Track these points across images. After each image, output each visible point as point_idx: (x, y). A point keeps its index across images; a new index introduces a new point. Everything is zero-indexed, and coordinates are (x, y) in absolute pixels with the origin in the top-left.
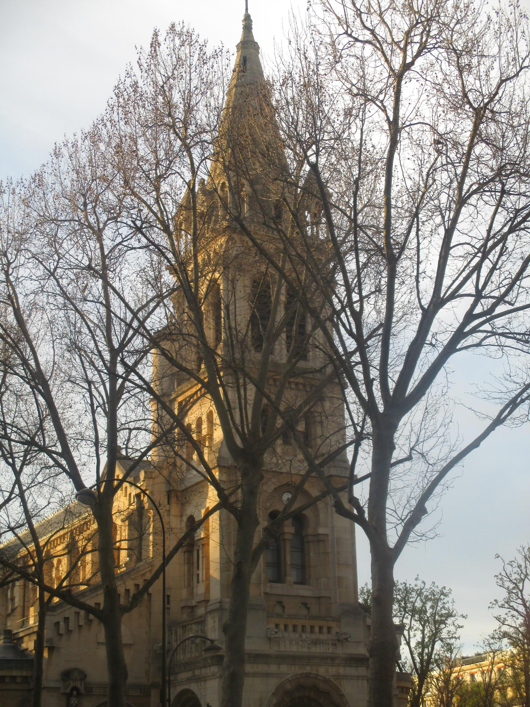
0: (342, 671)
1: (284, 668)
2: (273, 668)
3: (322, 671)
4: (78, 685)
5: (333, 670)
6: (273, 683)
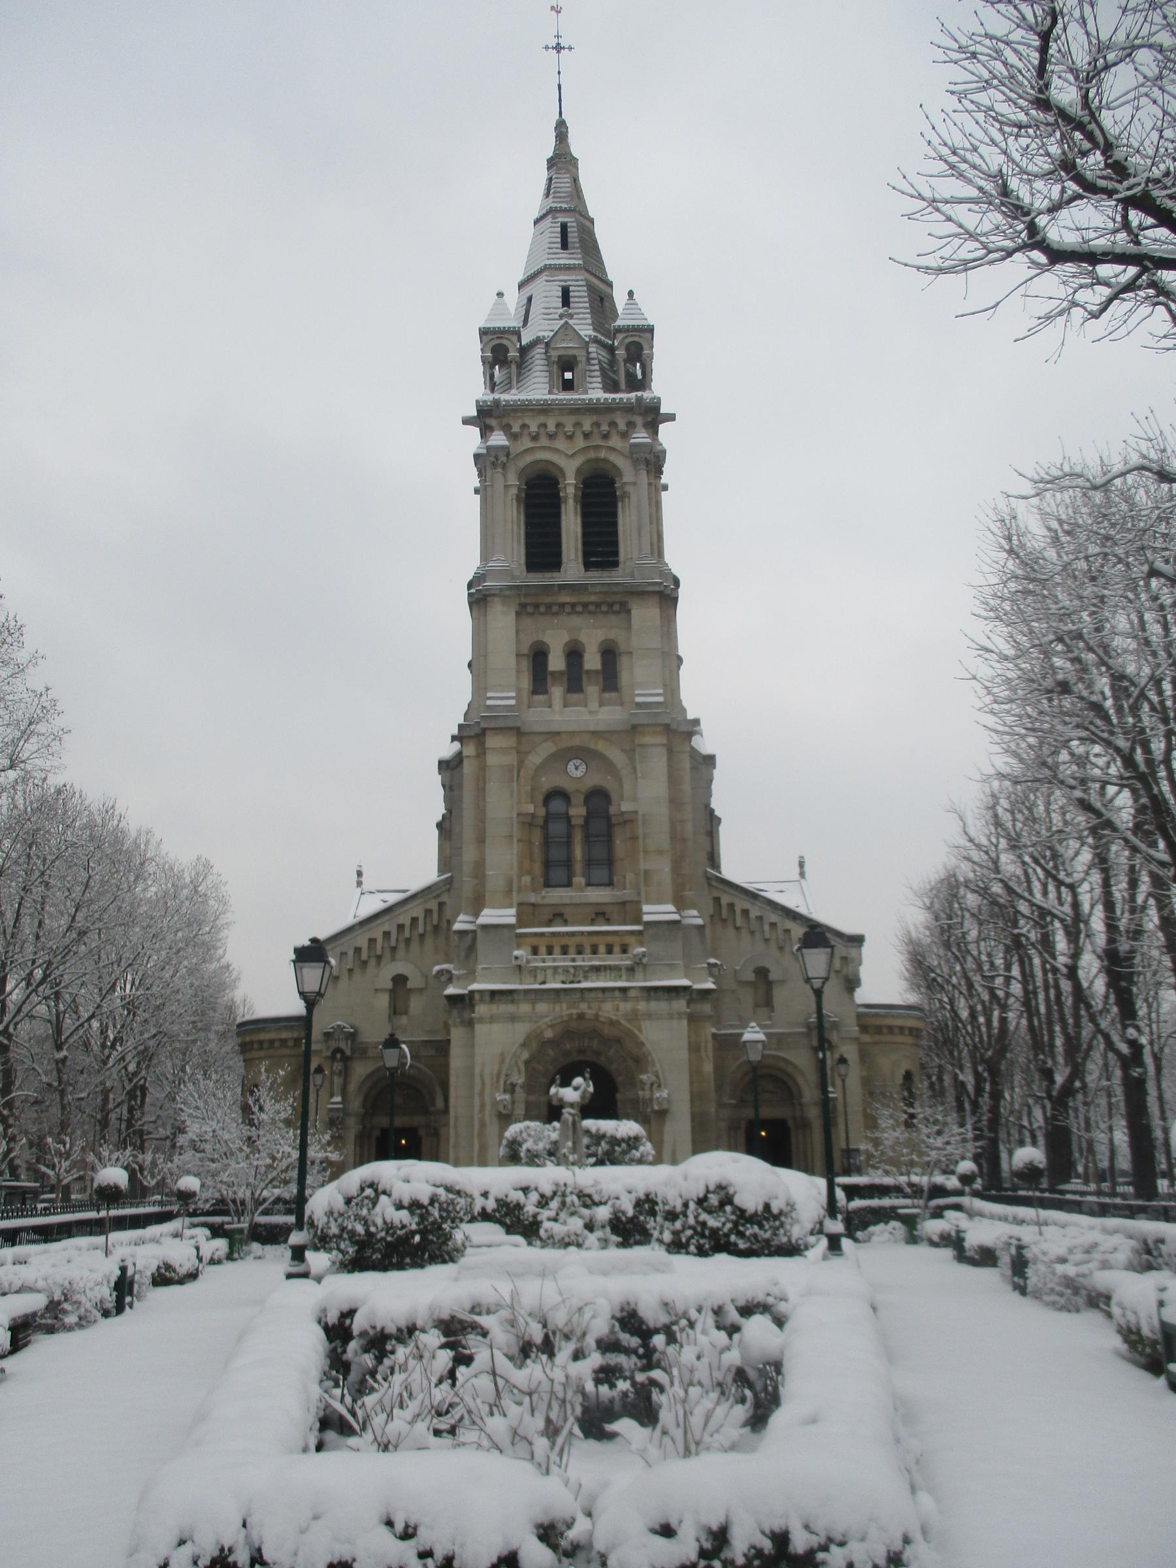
0: (642, 1006)
1: (542, 1007)
2: (525, 1008)
3: (608, 1009)
4: (343, 1045)
5: (625, 1007)
6: (522, 1030)
